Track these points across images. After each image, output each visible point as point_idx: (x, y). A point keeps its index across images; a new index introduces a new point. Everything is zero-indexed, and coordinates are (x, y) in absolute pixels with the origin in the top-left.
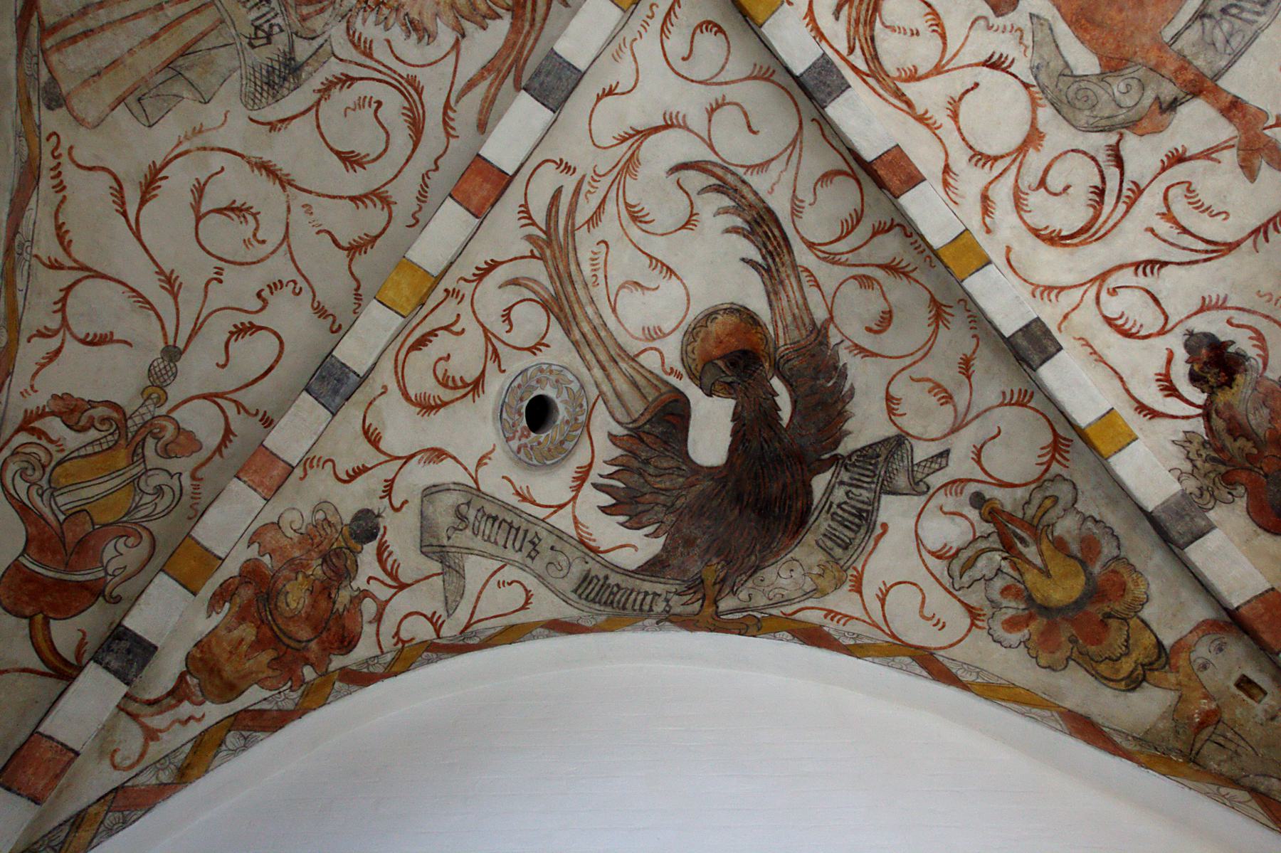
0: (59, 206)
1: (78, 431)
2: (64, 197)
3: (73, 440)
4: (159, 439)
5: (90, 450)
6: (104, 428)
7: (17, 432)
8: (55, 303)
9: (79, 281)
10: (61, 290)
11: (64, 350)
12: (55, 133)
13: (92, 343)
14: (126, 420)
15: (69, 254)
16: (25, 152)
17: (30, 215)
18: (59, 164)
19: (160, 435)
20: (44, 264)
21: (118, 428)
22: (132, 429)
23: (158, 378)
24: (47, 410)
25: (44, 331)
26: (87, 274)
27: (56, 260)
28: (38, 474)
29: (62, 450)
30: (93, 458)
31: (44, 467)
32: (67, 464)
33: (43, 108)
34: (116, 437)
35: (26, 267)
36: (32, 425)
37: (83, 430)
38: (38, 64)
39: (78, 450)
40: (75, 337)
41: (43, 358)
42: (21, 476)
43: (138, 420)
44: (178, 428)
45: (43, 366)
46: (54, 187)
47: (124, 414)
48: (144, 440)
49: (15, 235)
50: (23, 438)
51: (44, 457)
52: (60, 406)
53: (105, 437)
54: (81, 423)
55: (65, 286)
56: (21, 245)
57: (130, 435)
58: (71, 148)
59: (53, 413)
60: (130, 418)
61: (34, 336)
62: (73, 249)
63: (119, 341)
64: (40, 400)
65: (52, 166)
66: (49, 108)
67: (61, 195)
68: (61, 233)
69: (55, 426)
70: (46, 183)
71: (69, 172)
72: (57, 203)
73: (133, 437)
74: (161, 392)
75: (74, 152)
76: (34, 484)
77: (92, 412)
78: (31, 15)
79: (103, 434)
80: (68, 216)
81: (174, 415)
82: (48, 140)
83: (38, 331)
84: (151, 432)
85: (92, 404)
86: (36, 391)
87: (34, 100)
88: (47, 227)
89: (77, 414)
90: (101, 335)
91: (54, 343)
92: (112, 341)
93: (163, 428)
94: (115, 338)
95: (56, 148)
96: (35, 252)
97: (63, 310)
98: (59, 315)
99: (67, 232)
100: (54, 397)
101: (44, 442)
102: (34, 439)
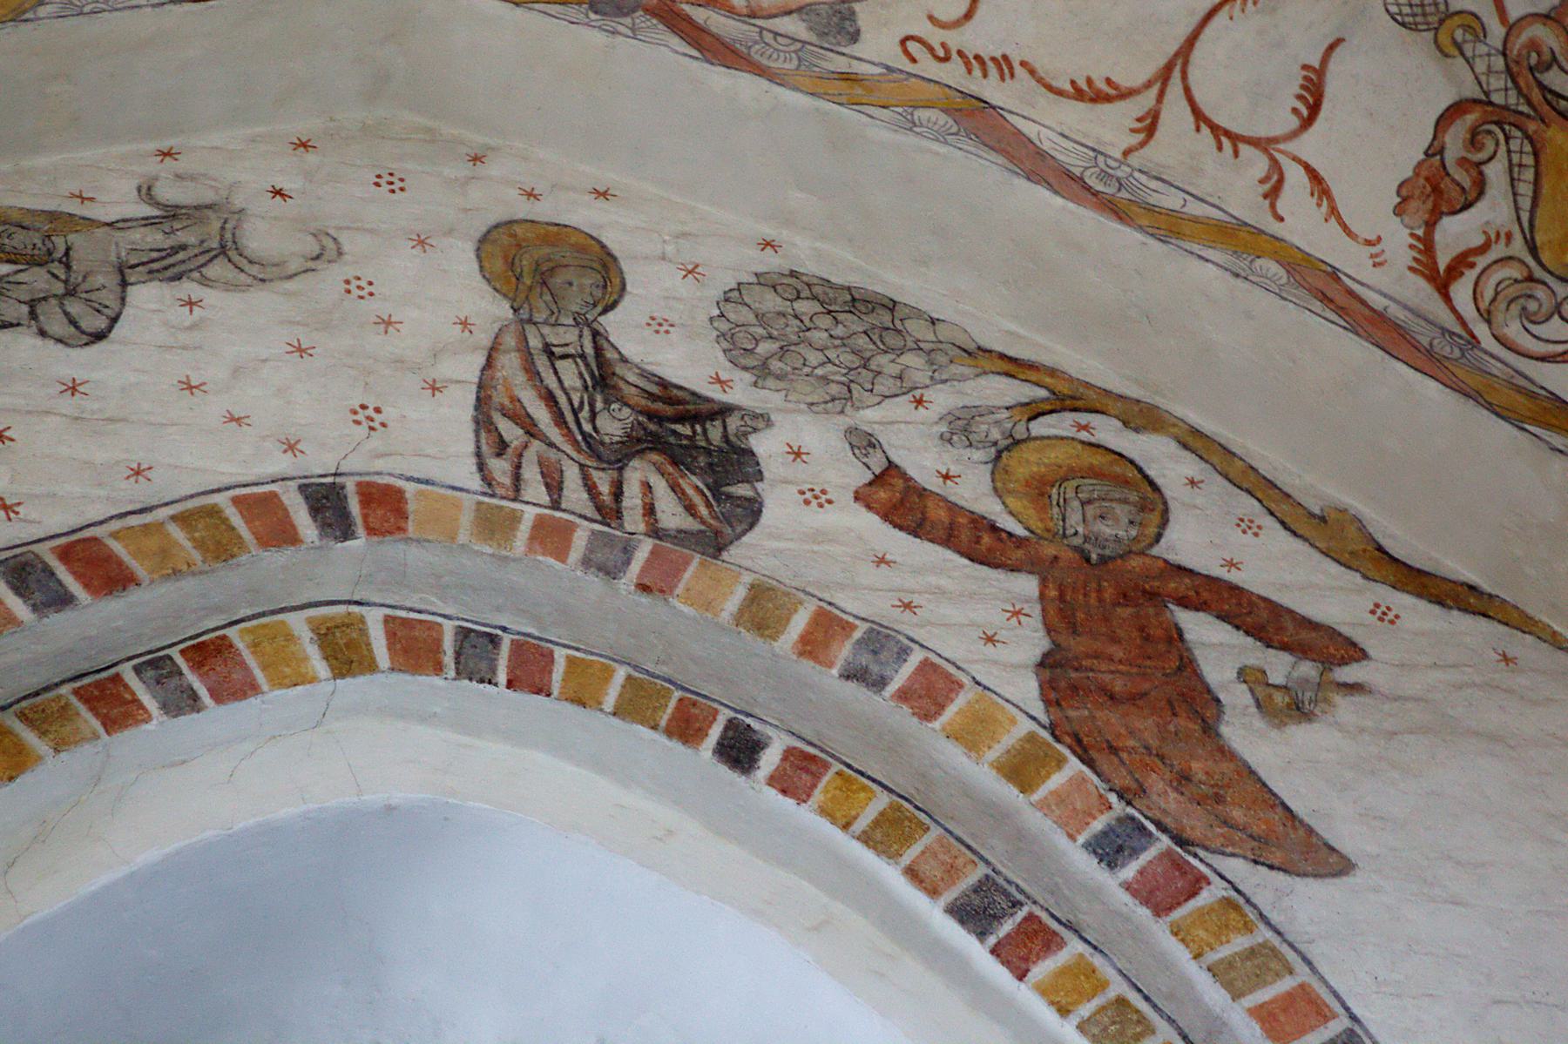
0: (1040, 81)
1: (1481, 193)
2: (1023, 64)
3: (1494, 210)
4: (1554, 59)
5: (1525, 189)
6: (1490, 146)
7: (1447, 298)
8: (1220, 148)
9: (1187, 91)
10: (1198, 129)
11: (1314, 164)
12: (903, 42)
13: (1315, 109)
14: (1490, 103)
15: (1129, 93)
16: (943, 119)
17: (1048, 141)
18: (960, 53)
19: (1547, 57)
20: (1143, 144)
21: (1498, 123)
22: (1512, 100)
23: (1424, 15)
24: (1420, 232)
25: (1267, 187)
26: (1177, 73)
27: (1139, 120)
28: (1540, 292)
29: (1509, 236)
30: (1546, 190)
31: (1530, 278)
32: (1539, 239)
33: (855, 50)
34: (1518, 134)
35: (1143, 179)
36: (1442, 271)
37: (1481, 185)
38: (776, 34)
39: (1517, 209)
40: (1294, 135)
41: (1319, 205)
42: (1534, 323)
43: (1497, 82)
44: (1546, 18)
45: (1334, 211)
46: (1002, 78)
47: (1475, 101)
48: (1543, 87)
49: (1088, 188)
50: (1462, 292)
51: (1514, 272)
52: (1419, 210)
53: (1509, 151)
54: (1467, 183)
55: (1191, 119)
56: (1105, 176)
57: (1524, 108)
58: (931, 18)
59: (1431, 225)
60: (1487, 94)
61: (1273, 206)
62: (1125, 80)
63: (1325, 60)
64: (1398, 239)
65: (963, 69)
66: (855, 37)
67: (1018, 70)
68: (1091, 94)
69: (1456, 232)
70: (992, 89)
71: (973, 39)
72: (1034, 83)
73: (1529, 103)
74: (1457, 20)
75: (942, 16)
76: (1557, 309)
77: (1451, 156)
78: (689, 20)
79: (1503, 148)
80: (1065, 67)
81: (1514, 13)
82: (914, 60)
83: (1266, 196)
84: (1531, 69)
85: (1435, 150)
86: (1379, 239)
87: (840, 64)
88: (1075, 115)
89: (1445, 184)
90: (1303, 87)
91: (1295, 177)
92: (1321, 72)
93: (1534, 45)
94: (1317, 65)
95: (931, 49)
96: (1118, 155)
97: (1235, 138)
98: (1244, 149)
99: (1089, 81)
100: (1399, 211)
101: (1482, 262)
102: (1470, 276)
